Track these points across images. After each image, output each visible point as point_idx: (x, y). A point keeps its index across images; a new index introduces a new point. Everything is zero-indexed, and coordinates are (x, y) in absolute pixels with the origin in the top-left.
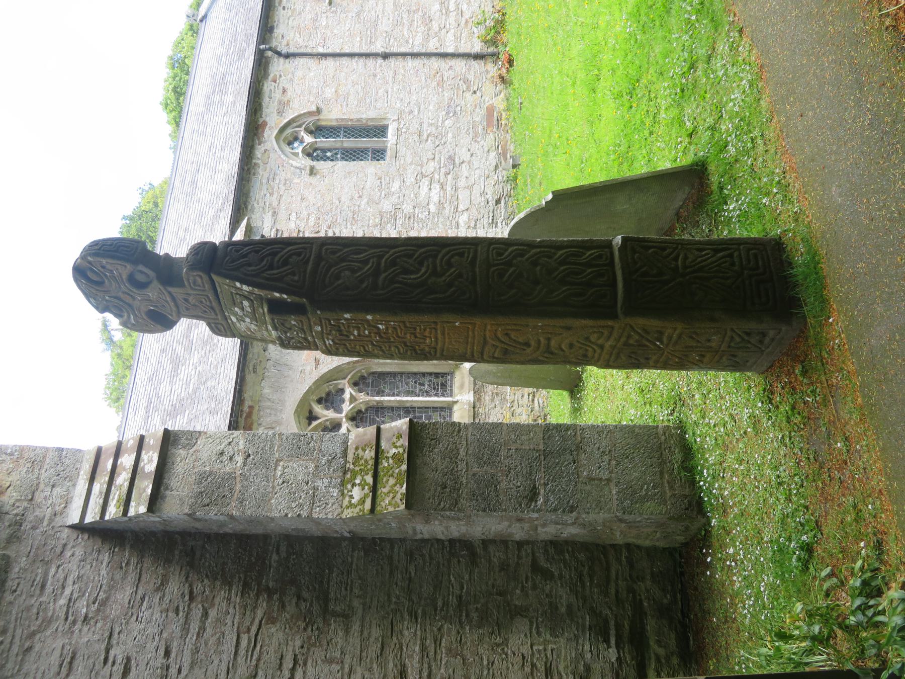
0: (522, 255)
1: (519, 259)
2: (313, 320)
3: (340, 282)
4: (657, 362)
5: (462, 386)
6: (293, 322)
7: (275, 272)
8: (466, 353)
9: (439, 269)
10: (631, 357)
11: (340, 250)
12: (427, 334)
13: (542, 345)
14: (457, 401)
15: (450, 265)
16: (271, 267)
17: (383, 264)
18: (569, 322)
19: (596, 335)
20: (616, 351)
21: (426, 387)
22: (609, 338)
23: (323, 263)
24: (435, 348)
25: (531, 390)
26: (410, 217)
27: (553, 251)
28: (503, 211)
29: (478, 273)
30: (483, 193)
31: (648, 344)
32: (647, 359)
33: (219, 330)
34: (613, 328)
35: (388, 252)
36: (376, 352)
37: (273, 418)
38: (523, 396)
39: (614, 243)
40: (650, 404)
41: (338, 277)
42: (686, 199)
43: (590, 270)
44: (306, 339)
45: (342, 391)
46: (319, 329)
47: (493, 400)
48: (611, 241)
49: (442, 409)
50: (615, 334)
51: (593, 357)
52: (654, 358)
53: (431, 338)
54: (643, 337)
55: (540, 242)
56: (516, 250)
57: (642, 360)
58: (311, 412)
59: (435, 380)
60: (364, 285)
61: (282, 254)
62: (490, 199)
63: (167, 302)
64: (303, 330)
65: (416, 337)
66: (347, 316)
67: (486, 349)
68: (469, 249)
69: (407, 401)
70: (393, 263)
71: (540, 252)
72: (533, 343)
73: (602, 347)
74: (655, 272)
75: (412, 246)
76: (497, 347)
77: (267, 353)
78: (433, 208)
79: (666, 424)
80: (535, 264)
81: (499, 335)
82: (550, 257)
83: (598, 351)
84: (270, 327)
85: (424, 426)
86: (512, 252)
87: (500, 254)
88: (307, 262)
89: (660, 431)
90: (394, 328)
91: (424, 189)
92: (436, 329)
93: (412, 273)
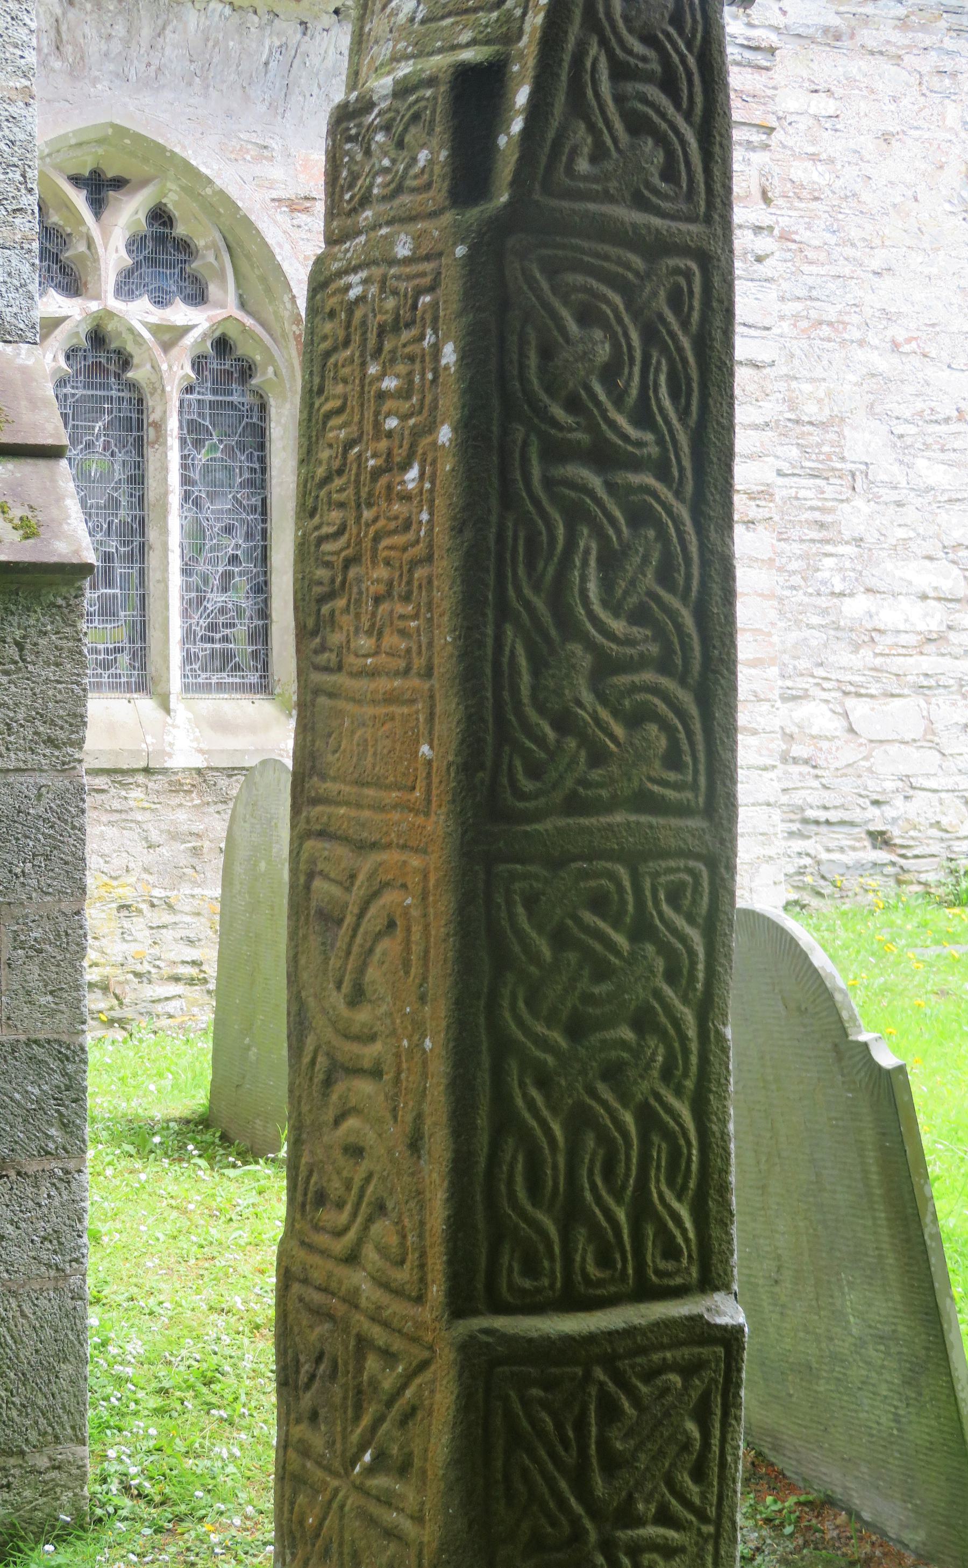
0: (672, 976)
1: (660, 965)
2: (434, 229)
3: (573, 327)
4: (305, 1451)
5: (222, 726)
6: (423, 156)
7: (605, 87)
8: (323, 777)
9: (623, 680)
10: (317, 1356)
11: (685, 324)
12: (391, 640)
13: (355, 1048)
14: (167, 710)
15: (636, 719)
16: (620, 72)
17: (636, 479)
18: (439, 1144)
19: (394, 1240)
20: (340, 1308)
21: (216, 599)
22: (384, 1285)
23: (637, 261)
24: (340, 668)
25: (211, 970)
26: (822, 525)
27: (689, 1084)
28: (849, 858)
29: (605, 820)
30: (910, 787)
31: (366, 1421)
32: (314, 1417)
34: (419, 1299)
35: (678, 494)
36: (325, 454)
37: (95, 47)
38: (190, 942)
39: (719, 1298)
40: (160, 1412)
41: (587, 316)
42: (884, 1534)
43: (621, 1215)
44: (365, 201)
45: (198, 297)
47: (175, 836)
48: (727, 1287)
49: (140, 657)
50: (396, 1308)
51: (317, 1228)
52: (318, 1442)
53: (376, 653)
54: (390, 1403)
55: (720, 1037)
56: (692, 953)
57: (307, 1400)
58: (119, 183)
59: (241, 629)
60: (559, 413)
61: (671, 110)
62: (889, 812)
64: (399, 190)
65: (378, 600)
66: (449, 355)
67: (341, 850)
68: (695, 787)
69: (165, 531)
70: (639, 516)
71: (683, 1038)
72: (363, 1016)
73: (352, 1258)
74: (619, 1445)
75: (703, 584)
76: (348, 889)
77: (328, 20)
78: (856, 607)
79: (92, 1471)
80: (643, 1022)
81: (389, 898)
82: (667, 1074)
83: (340, 1246)
84: (405, 69)
85: (68, 613)
86: (683, 939)
87: (674, 898)
88: (640, 202)
89: (68, 1451)
91: (925, 577)
92: (407, 672)
93: (607, 585)
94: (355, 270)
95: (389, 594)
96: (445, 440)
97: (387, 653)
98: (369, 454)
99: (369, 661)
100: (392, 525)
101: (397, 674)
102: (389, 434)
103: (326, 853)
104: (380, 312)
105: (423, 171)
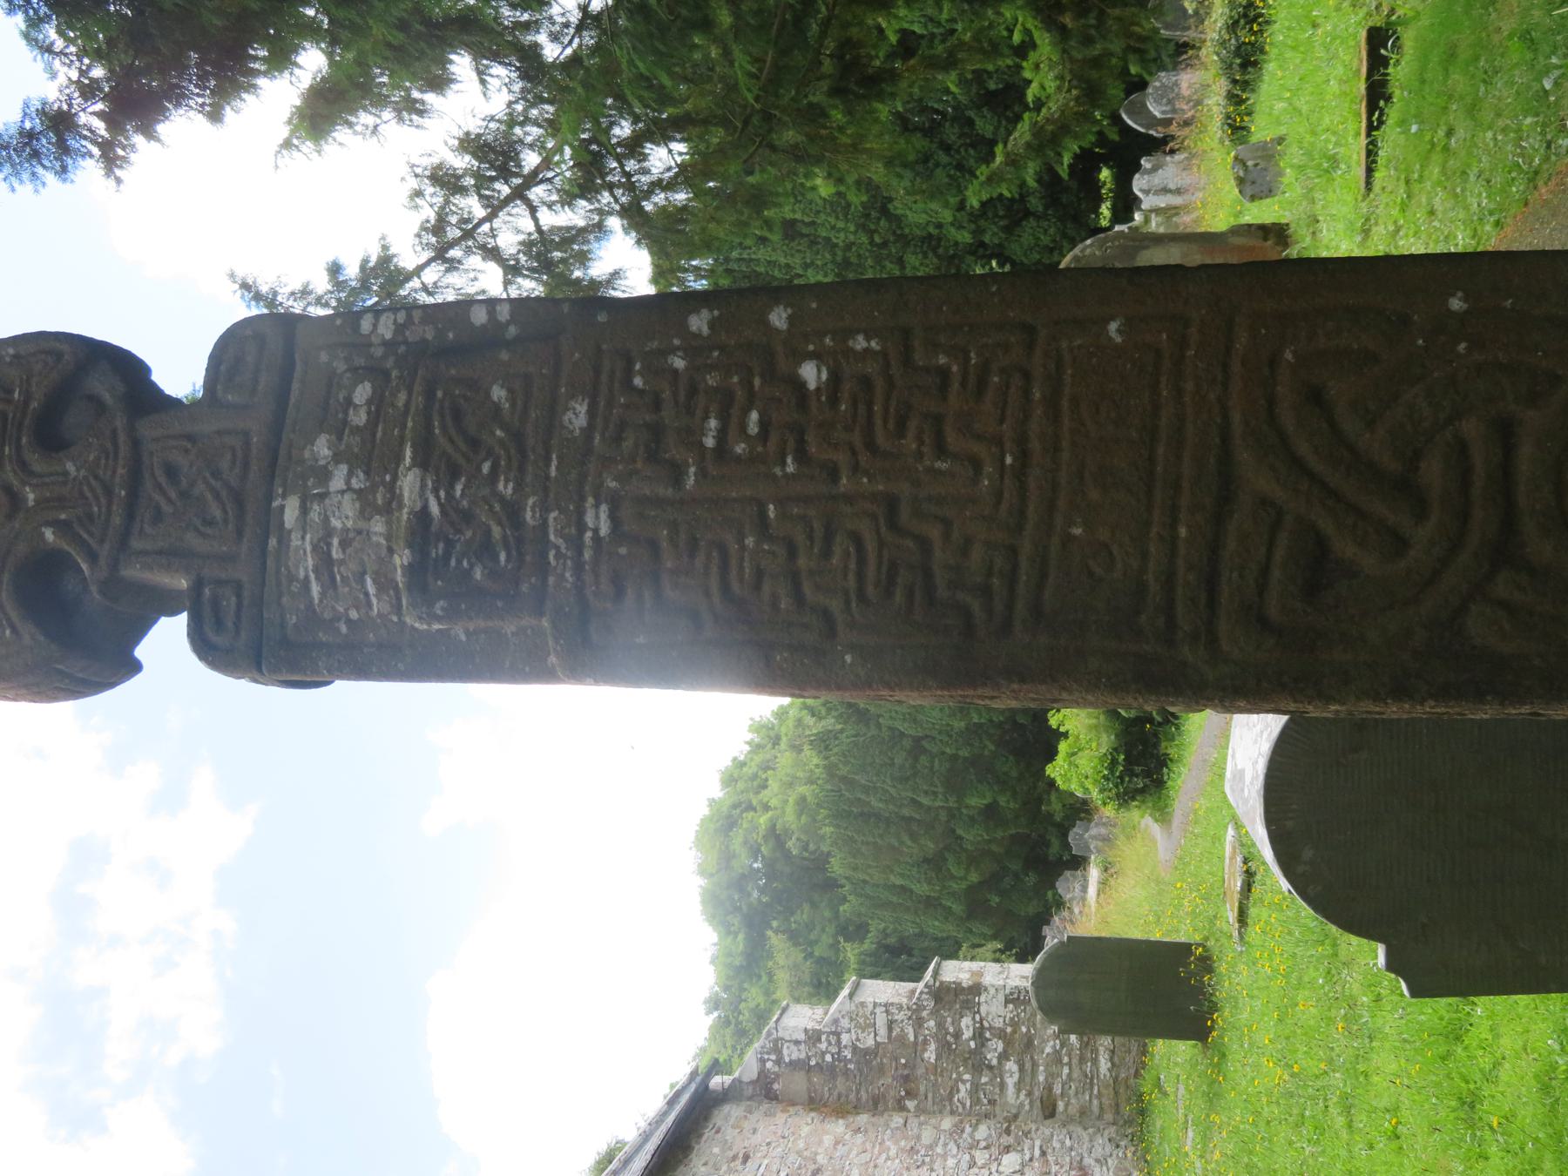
6: (498, 393)
24: (1013, 551)
33: (219, 624)
46: (577, 416)
53: (998, 441)
63: (109, 492)
72: (1433, 472)
90: (866, 382)
92: (1027, 376)
94: (582, 528)
95: (938, 419)
96: (784, 315)
97: (1002, 421)
98: (778, 471)
99: (1009, 460)
100: (862, 409)
101: (1027, 393)
102: (764, 424)
103: (1235, 575)
104: (634, 461)
105: (511, 391)
